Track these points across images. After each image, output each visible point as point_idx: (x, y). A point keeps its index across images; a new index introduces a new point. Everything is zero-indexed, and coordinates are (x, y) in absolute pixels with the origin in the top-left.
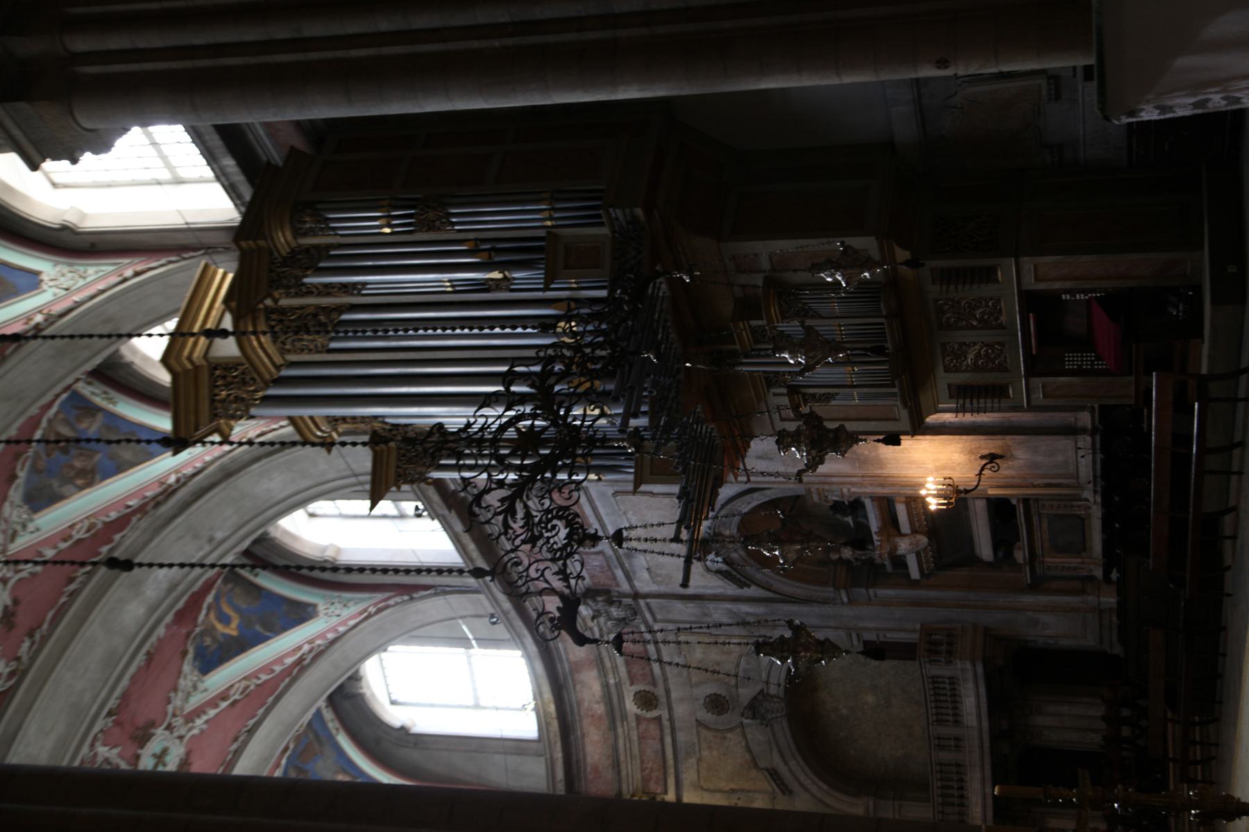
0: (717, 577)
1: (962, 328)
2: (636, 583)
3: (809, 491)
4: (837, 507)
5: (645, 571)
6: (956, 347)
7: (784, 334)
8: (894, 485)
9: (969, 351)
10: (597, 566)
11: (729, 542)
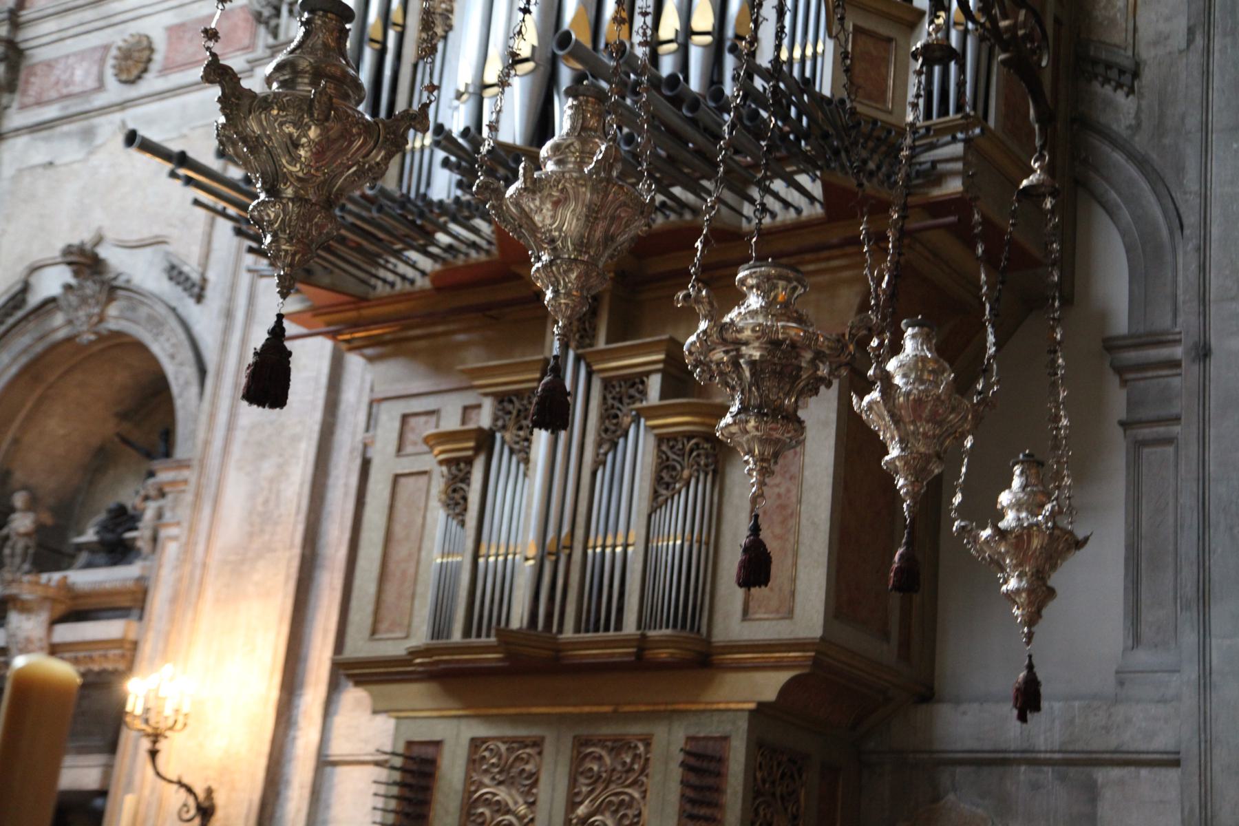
0: (17, 283)
1: (573, 782)
2: (21, 142)
3: (184, 465)
4: (123, 518)
5: (47, 159)
6: (528, 767)
7: (619, 437)
8: (172, 620)
9: (514, 792)
10: (72, 74)
11: (90, 316)
